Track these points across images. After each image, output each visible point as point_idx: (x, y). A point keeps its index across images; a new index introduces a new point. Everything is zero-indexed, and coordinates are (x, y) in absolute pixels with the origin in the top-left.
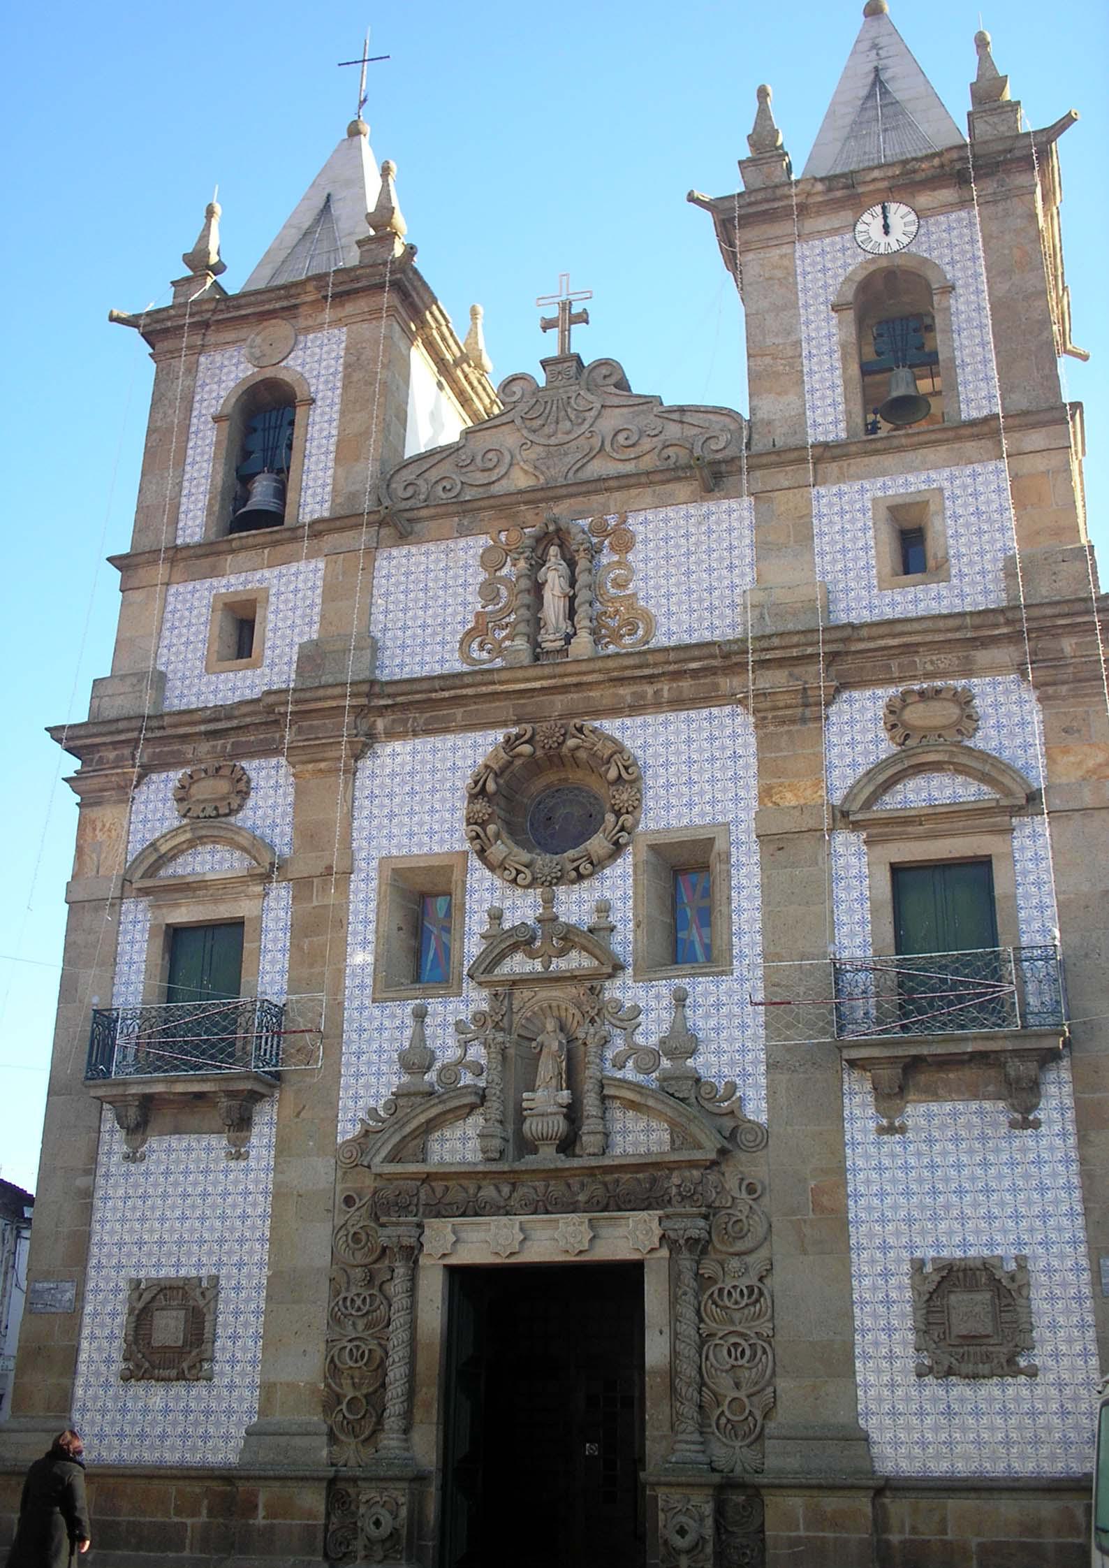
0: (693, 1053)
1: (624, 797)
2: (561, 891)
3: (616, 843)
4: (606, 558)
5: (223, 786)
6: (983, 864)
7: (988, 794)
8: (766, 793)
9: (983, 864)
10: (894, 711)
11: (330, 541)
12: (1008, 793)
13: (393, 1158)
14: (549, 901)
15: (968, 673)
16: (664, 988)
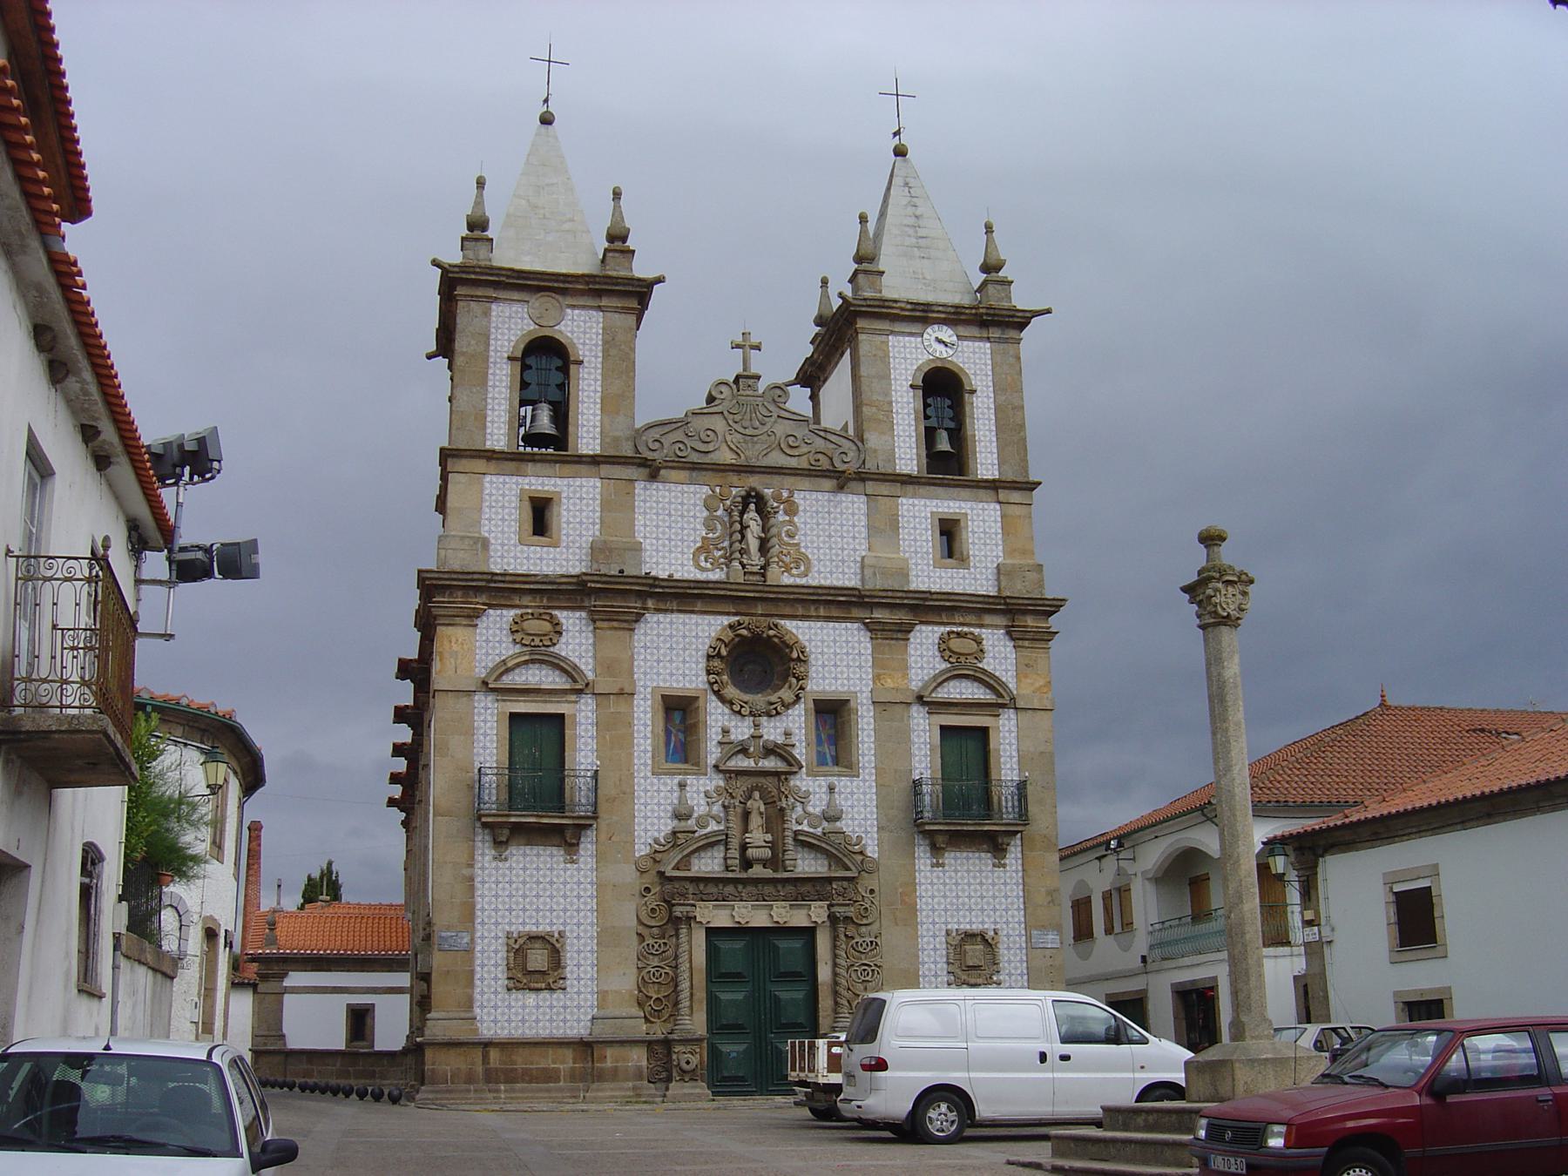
0: (838, 819)
1: (800, 669)
2: (764, 719)
3: (797, 696)
4: (781, 517)
5: (547, 627)
6: (984, 731)
7: (989, 697)
8: (877, 678)
9: (984, 731)
10: (943, 640)
11: (605, 470)
12: (1000, 695)
13: (676, 868)
14: (756, 726)
15: (981, 626)
16: (823, 782)
